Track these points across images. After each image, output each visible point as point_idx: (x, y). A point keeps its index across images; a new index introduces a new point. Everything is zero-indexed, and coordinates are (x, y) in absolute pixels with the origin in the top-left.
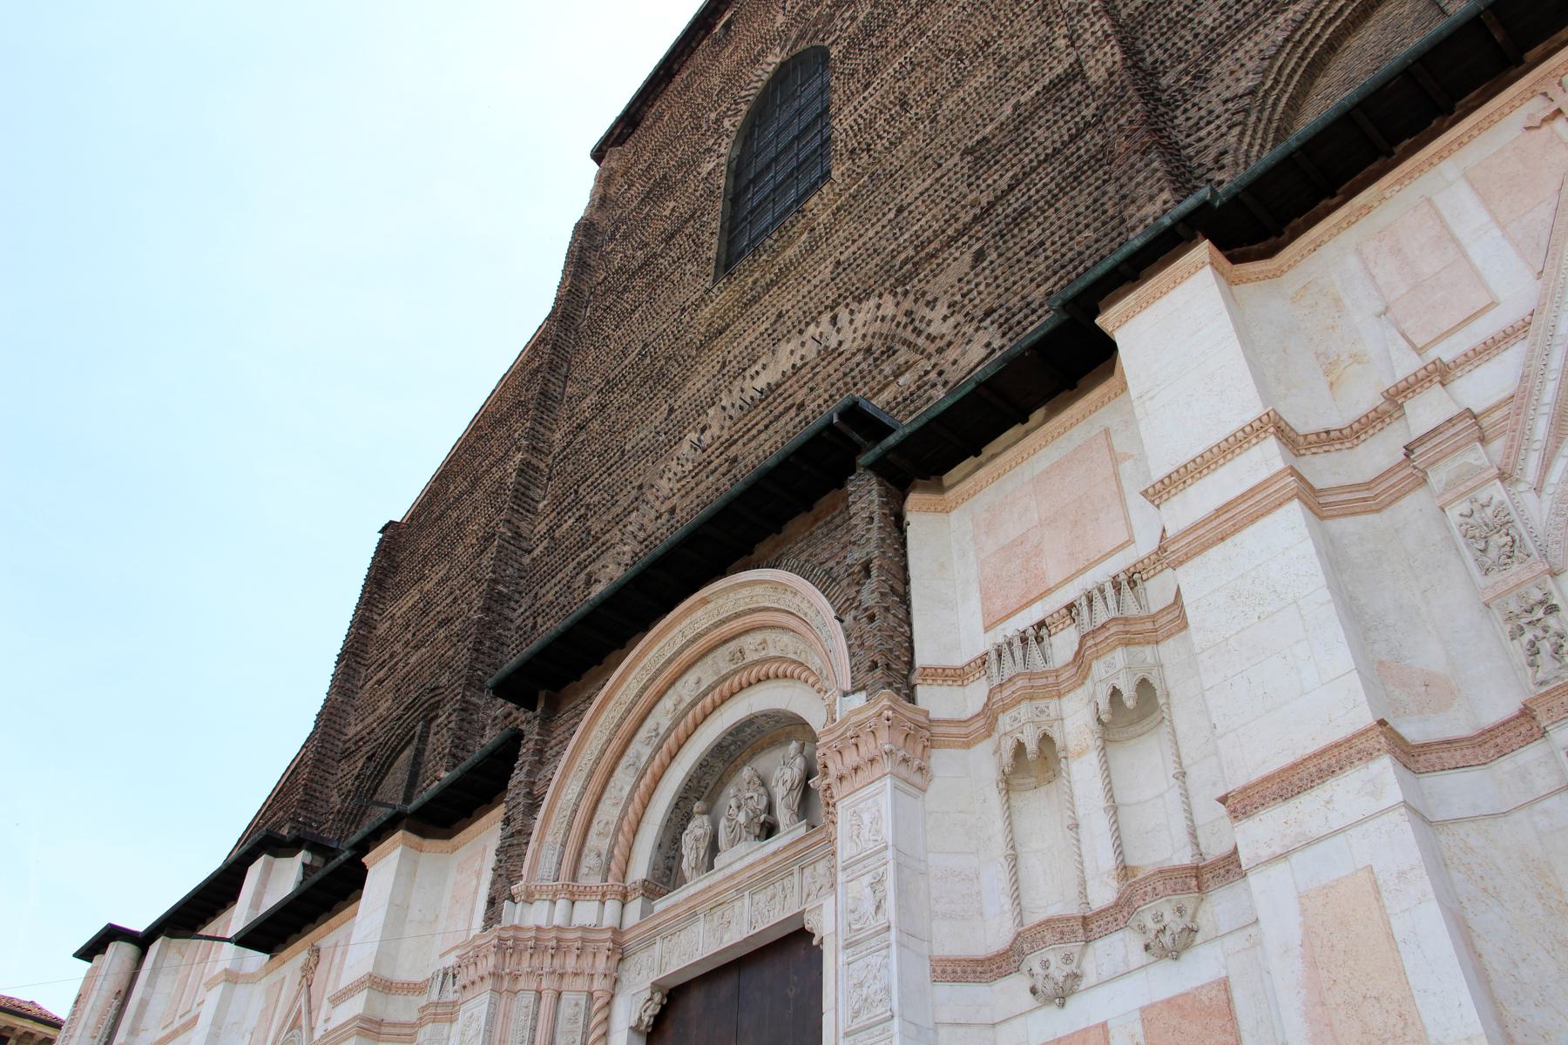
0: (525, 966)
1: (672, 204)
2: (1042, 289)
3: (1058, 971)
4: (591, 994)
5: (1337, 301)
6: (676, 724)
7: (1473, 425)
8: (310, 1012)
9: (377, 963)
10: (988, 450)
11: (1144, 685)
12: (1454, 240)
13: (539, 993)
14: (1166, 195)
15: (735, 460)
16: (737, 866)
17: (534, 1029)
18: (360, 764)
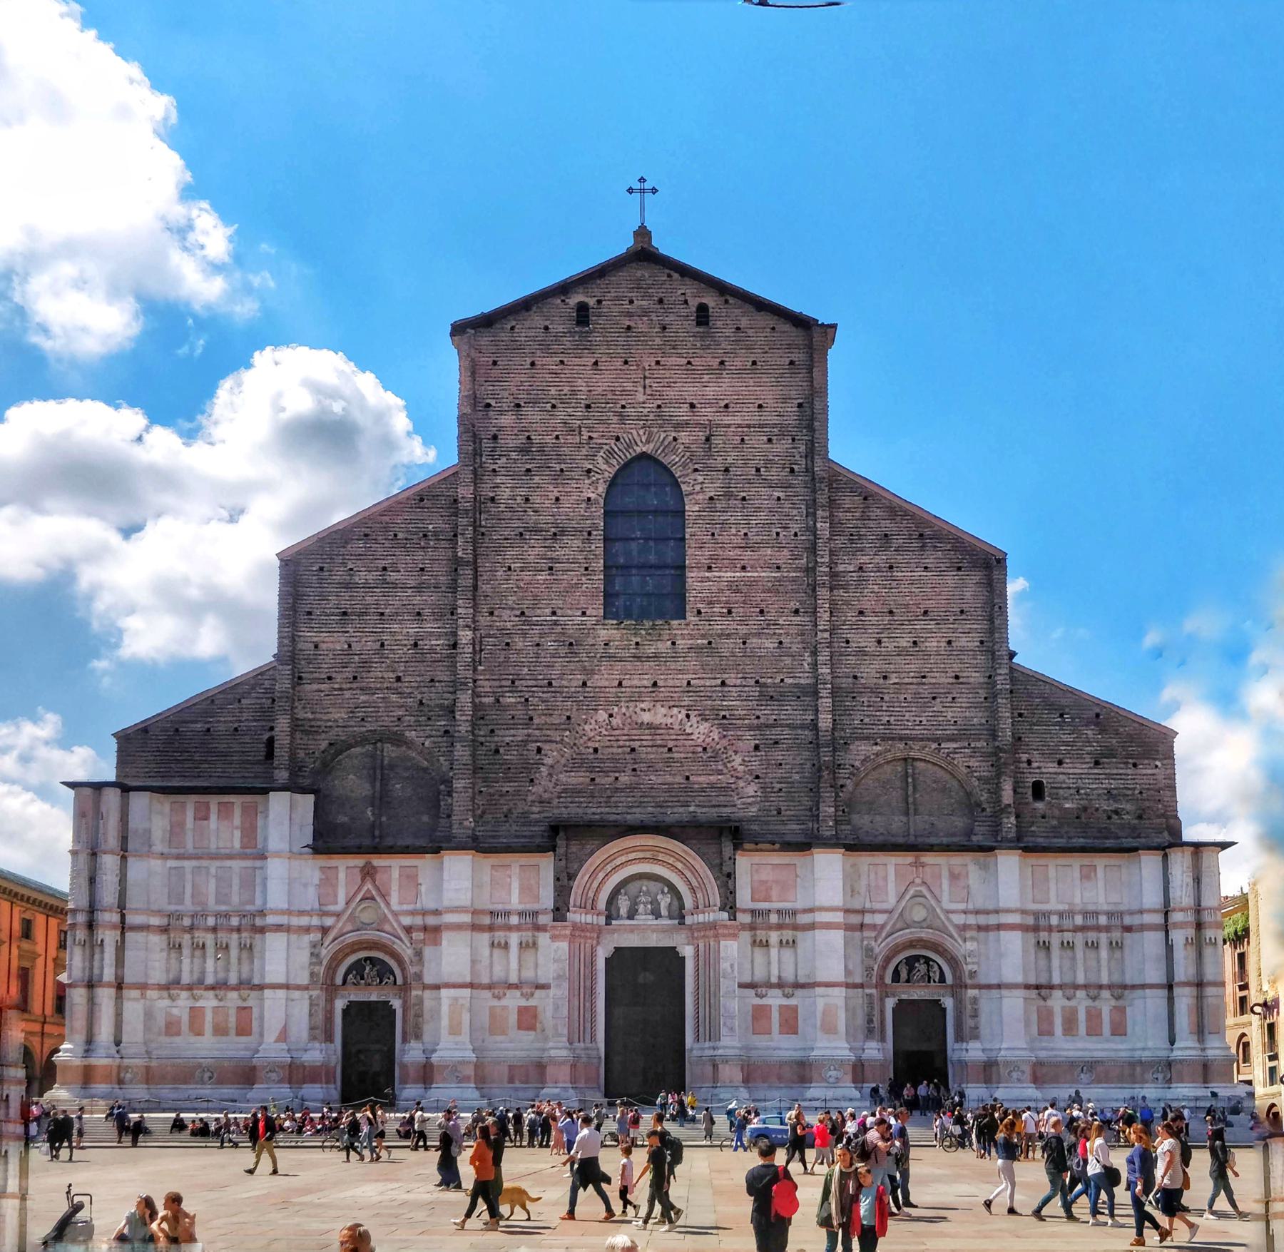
1: (558, 494)
2: (779, 786)
3: (764, 993)
5: (859, 876)
7: (873, 927)
11: (794, 941)
15: (633, 750)
18: (324, 745)
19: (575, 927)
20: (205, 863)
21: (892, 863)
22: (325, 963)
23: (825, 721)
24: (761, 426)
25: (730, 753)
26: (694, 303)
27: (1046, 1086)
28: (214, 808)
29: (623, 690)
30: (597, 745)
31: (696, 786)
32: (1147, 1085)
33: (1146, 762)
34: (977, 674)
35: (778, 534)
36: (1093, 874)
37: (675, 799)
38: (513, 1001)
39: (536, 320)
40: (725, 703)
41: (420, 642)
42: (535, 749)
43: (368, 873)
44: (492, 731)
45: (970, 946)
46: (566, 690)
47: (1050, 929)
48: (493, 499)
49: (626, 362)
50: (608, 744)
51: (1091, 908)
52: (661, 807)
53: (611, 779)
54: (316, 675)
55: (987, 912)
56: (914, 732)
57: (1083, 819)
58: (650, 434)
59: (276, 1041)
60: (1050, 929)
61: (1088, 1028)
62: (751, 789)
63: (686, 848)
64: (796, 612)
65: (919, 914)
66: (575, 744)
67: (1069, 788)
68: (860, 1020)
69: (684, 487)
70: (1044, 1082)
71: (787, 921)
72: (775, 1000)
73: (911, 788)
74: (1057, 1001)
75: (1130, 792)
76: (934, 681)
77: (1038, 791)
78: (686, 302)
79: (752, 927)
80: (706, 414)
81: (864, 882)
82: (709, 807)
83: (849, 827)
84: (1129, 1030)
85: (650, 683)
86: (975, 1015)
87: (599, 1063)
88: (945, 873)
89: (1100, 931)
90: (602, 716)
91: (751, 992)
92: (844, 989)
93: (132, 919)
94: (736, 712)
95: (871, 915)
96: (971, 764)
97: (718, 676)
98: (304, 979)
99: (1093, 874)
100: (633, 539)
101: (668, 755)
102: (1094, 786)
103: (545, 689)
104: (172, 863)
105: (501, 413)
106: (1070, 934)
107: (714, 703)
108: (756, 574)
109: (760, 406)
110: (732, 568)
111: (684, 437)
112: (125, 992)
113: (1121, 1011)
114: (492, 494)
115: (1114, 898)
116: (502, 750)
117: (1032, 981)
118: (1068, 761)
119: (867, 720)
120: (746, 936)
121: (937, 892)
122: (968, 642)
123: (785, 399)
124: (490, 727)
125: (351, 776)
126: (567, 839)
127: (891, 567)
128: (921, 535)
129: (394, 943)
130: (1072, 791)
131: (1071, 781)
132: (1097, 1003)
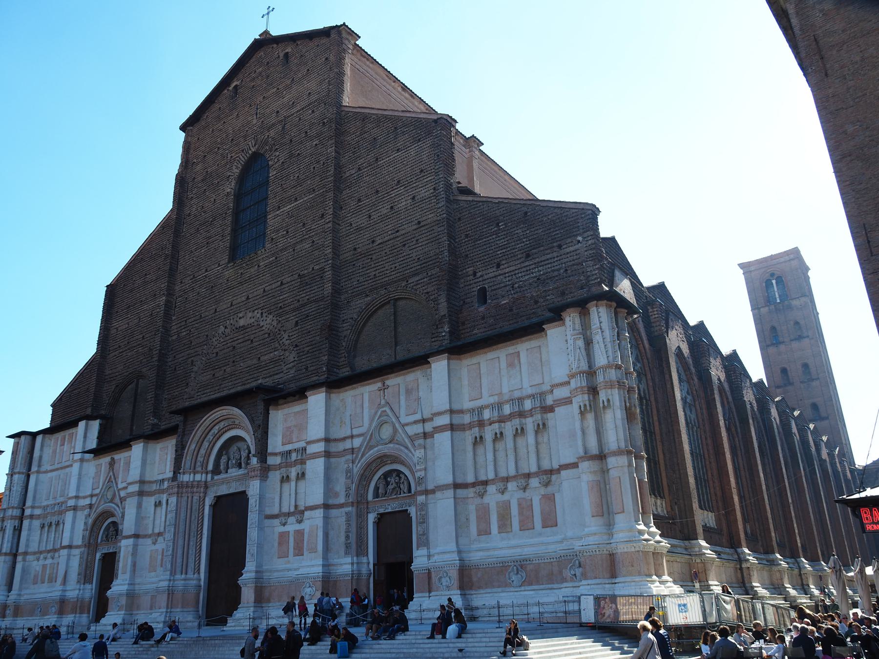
0: (184, 490)
1: (214, 198)
3: (284, 521)
4: (200, 497)
5: (346, 407)
6: (218, 432)
8: (115, 479)
9: (141, 476)
10: (289, 399)
12: (363, 407)
13: (188, 497)
14: (326, 357)
15: (234, 347)
16: (233, 474)
17: (187, 505)
18: (113, 387)
19: (181, 486)
20: (59, 472)
21: (367, 391)
22: (89, 529)
23: (328, 287)
24: (309, 105)
25: (283, 333)
26: (282, 55)
27: (482, 591)
28: (67, 437)
29: (232, 307)
30: (217, 350)
31: (263, 363)
32: (565, 585)
33: (569, 240)
34: (432, 215)
35: (314, 168)
36: (516, 361)
37: (252, 376)
38: (161, 545)
39: (216, 106)
40: (281, 298)
41: (153, 312)
42: (190, 362)
43: (112, 463)
44: (175, 357)
45: (419, 453)
46: (207, 318)
47: (481, 424)
48: (189, 215)
49: (250, 106)
50: (223, 348)
51: (517, 394)
52: (244, 384)
53: (221, 372)
54: (115, 347)
55: (431, 419)
56: (391, 277)
57: (515, 311)
58: (257, 141)
59: (61, 585)
60: (481, 424)
61: (520, 522)
62: (292, 357)
63: (240, 412)
64: (323, 215)
65: (386, 432)
66: (208, 353)
67: (505, 286)
68: (342, 539)
69: (270, 163)
70: (480, 588)
71: (299, 458)
72: (292, 527)
73: (393, 325)
74: (492, 497)
75: (556, 273)
76: (403, 232)
77: (483, 296)
78: (279, 57)
79: (279, 467)
80: (284, 113)
81: (348, 414)
82: (268, 377)
83: (348, 369)
84: (560, 520)
85: (244, 299)
86: (424, 520)
87: (200, 591)
88: (403, 391)
89: (526, 417)
90: (222, 328)
91: (276, 522)
92: (322, 510)
93: (28, 512)
94: (286, 302)
95: (350, 440)
96: (429, 290)
97: (279, 279)
98: (78, 541)
99: (516, 361)
100: (248, 208)
101: (251, 346)
102: (527, 277)
103: (198, 321)
104: (49, 475)
105: (197, 164)
106: (497, 424)
107: (276, 300)
108: (302, 200)
109: (310, 93)
110: (290, 202)
111: (272, 133)
112: (19, 558)
113: (550, 499)
114: (189, 212)
115: (537, 380)
116: (177, 367)
117: (470, 479)
118: (504, 262)
119: (360, 281)
120: (275, 477)
121: (396, 410)
122: (424, 193)
123: (321, 83)
124: (174, 355)
125: (126, 404)
126: (185, 422)
127: (377, 159)
128: (395, 128)
129: (115, 510)
130: (508, 288)
131: (507, 279)
132: (528, 491)
